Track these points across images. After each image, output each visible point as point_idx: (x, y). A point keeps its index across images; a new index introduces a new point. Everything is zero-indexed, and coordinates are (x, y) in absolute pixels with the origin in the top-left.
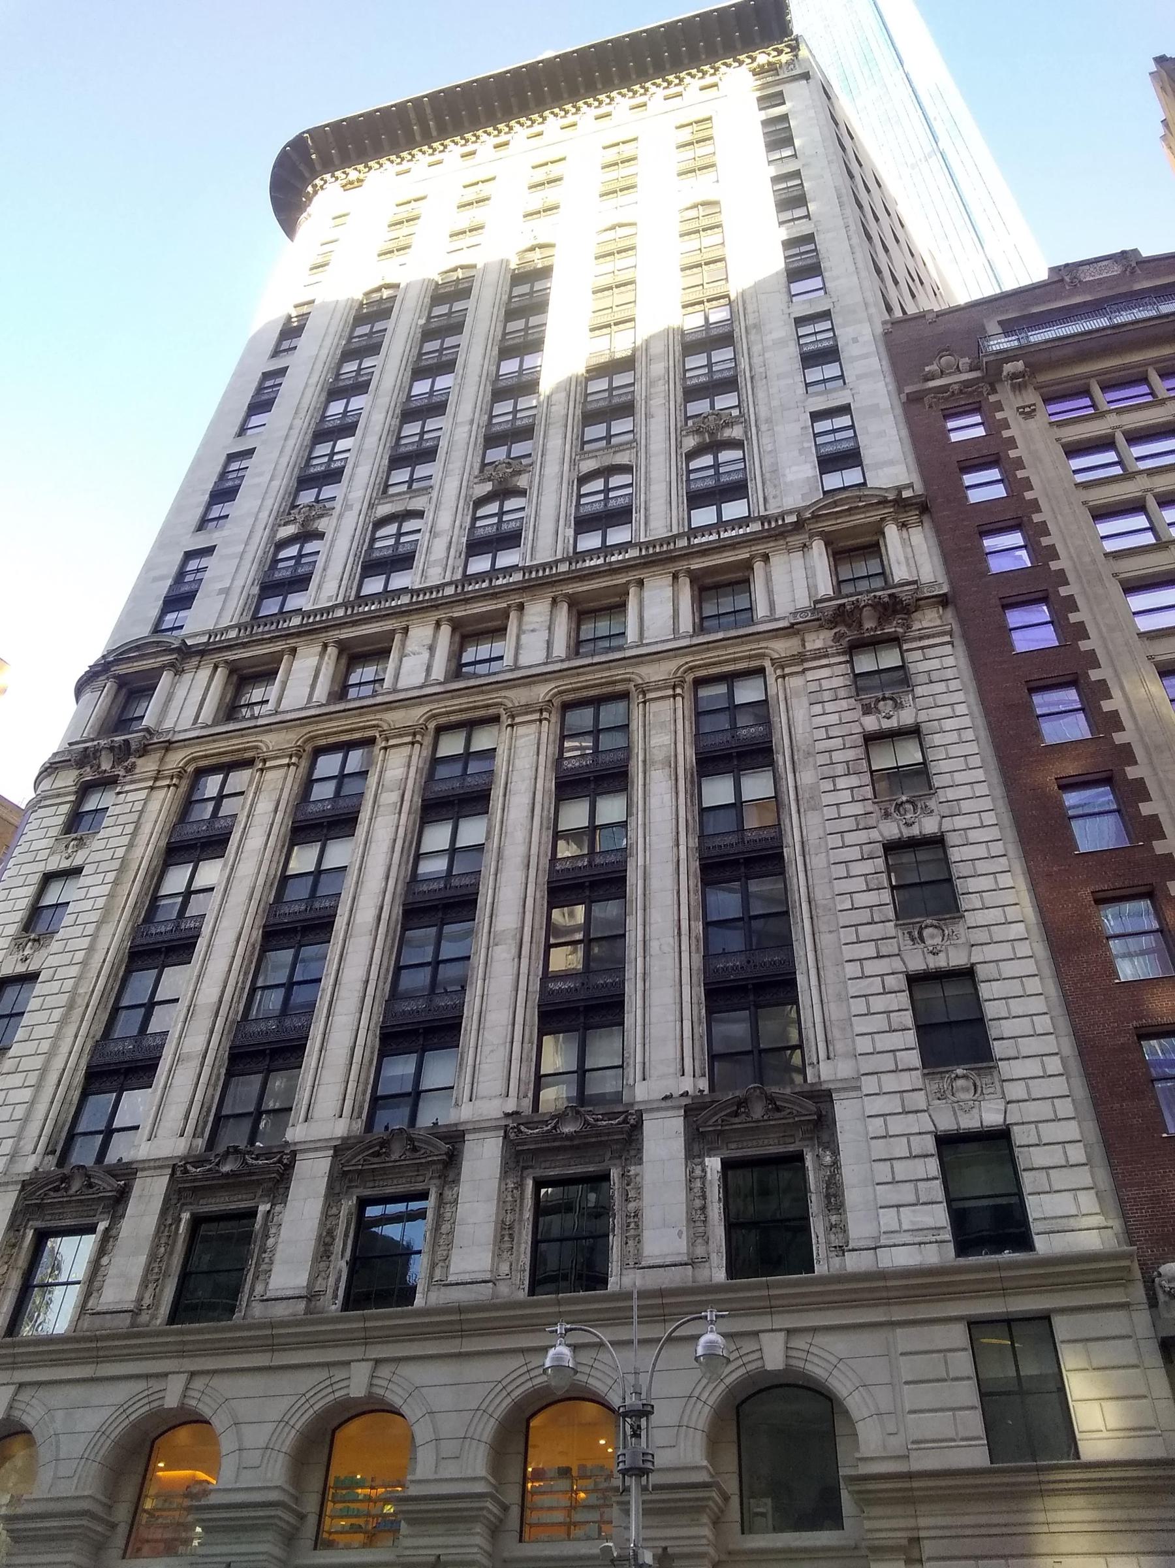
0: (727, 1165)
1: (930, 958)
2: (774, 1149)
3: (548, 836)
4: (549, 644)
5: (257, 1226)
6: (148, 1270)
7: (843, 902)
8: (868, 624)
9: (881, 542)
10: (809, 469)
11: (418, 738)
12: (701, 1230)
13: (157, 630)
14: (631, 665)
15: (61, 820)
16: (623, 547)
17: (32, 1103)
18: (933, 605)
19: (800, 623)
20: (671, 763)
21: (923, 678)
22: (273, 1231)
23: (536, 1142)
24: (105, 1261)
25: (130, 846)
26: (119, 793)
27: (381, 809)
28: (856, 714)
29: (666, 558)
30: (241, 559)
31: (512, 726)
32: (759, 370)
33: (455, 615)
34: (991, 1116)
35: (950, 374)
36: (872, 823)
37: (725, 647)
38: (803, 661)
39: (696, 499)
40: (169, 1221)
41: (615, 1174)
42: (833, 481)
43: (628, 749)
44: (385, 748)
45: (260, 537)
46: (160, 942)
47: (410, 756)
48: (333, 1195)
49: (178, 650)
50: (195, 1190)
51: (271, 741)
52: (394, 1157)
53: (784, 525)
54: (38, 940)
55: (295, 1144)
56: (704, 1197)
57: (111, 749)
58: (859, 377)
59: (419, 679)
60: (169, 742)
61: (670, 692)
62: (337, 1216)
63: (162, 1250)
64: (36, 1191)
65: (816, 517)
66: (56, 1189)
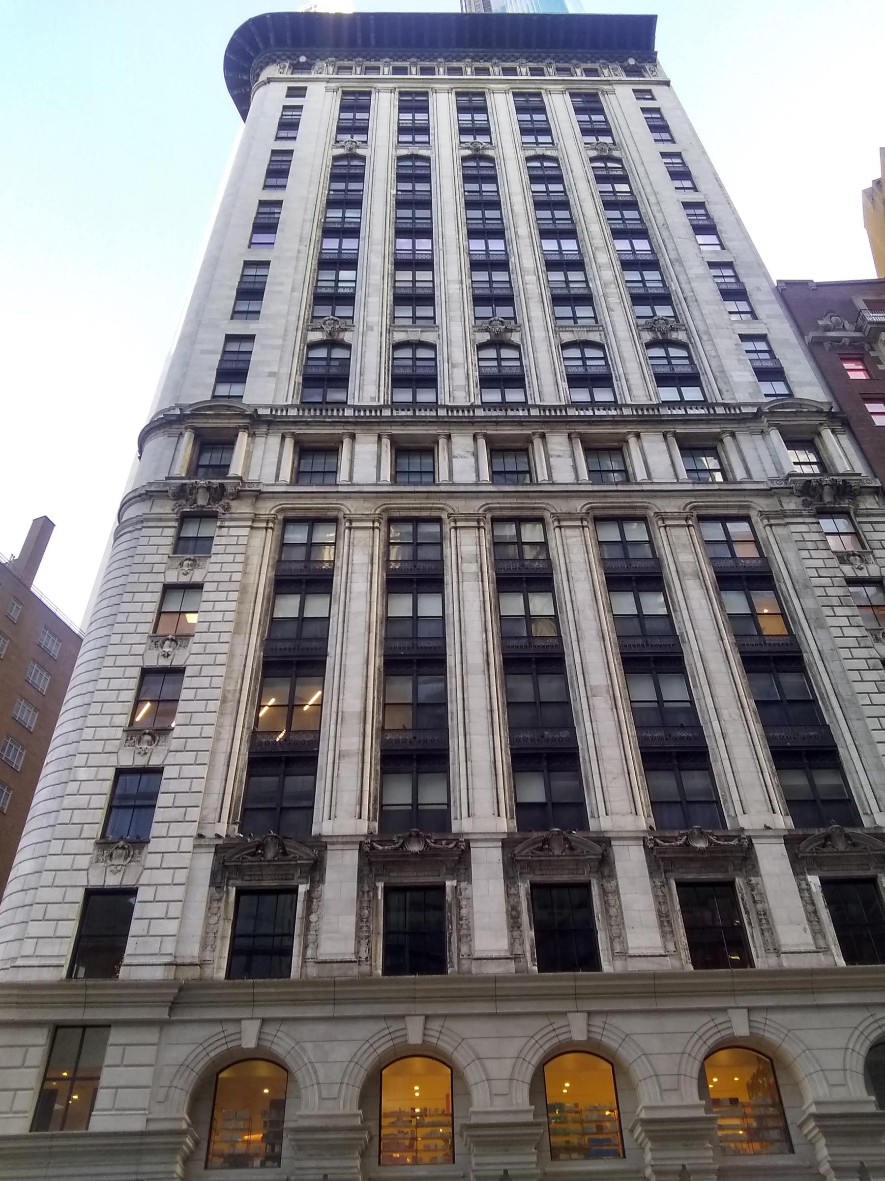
0: (824, 882)
2: (857, 873)
3: (610, 618)
5: (449, 897)
6: (359, 929)
7: (862, 699)
8: (827, 499)
9: (817, 441)
10: (749, 376)
12: (817, 928)
13: (214, 397)
14: (647, 497)
15: (170, 541)
16: (606, 405)
17: (208, 779)
18: (870, 494)
19: (777, 488)
20: (699, 575)
21: (878, 545)
22: (463, 903)
23: (674, 853)
24: (313, 918)
25: (245, 573)
26: (221, 527)
27: (465, 576)
28: (836, 562)
29: (657, 421)
30: (282, 351)
31: (560, 527)
33: (489, 432)
35: (839, 330)
36: (870, 644)
37: (720, 496)
38: (786, 517)
39: (662, 380)
40: (366, 888)
41: (739, 881)
42: (767, 387)
43: (657, 560)
46: (293, 658)
47: (479, 538)
48: (510, 879)
49: (250, 416)
50: (385, 865)
51: (351, 507)
52: (557, 852)
53: (741, 413)
54: (175, 641)
55: (467, 834)
56: (813, 904)
57: (208, 488)
58: (769, 317)
59: (472, 478)
60: (260, 492)
62: (517, 895)
63: (366, 912)
64: (232, 857)
65: (771, 413)
66: (254, 854)
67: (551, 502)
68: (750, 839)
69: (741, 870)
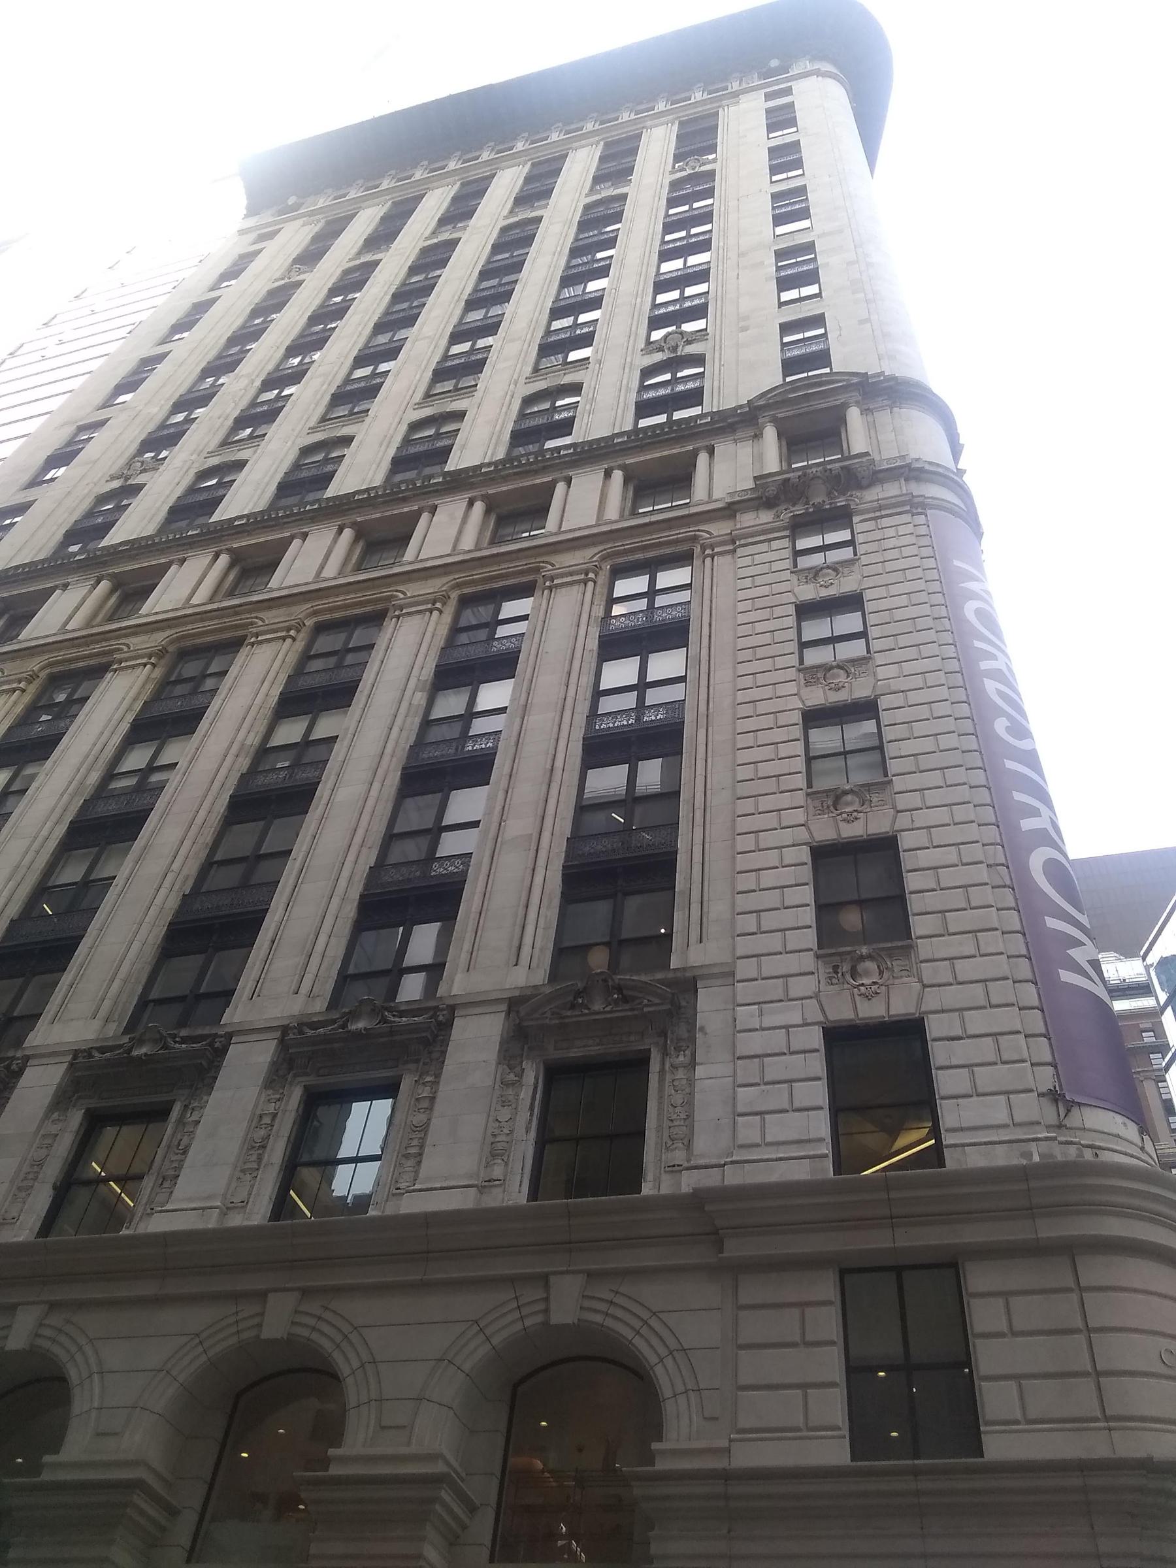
1: (842, 825)
11: (292, 633)
34: (900, 1003)
44: (253, 644)
68: (452, 1009)
69: (417, 1061)
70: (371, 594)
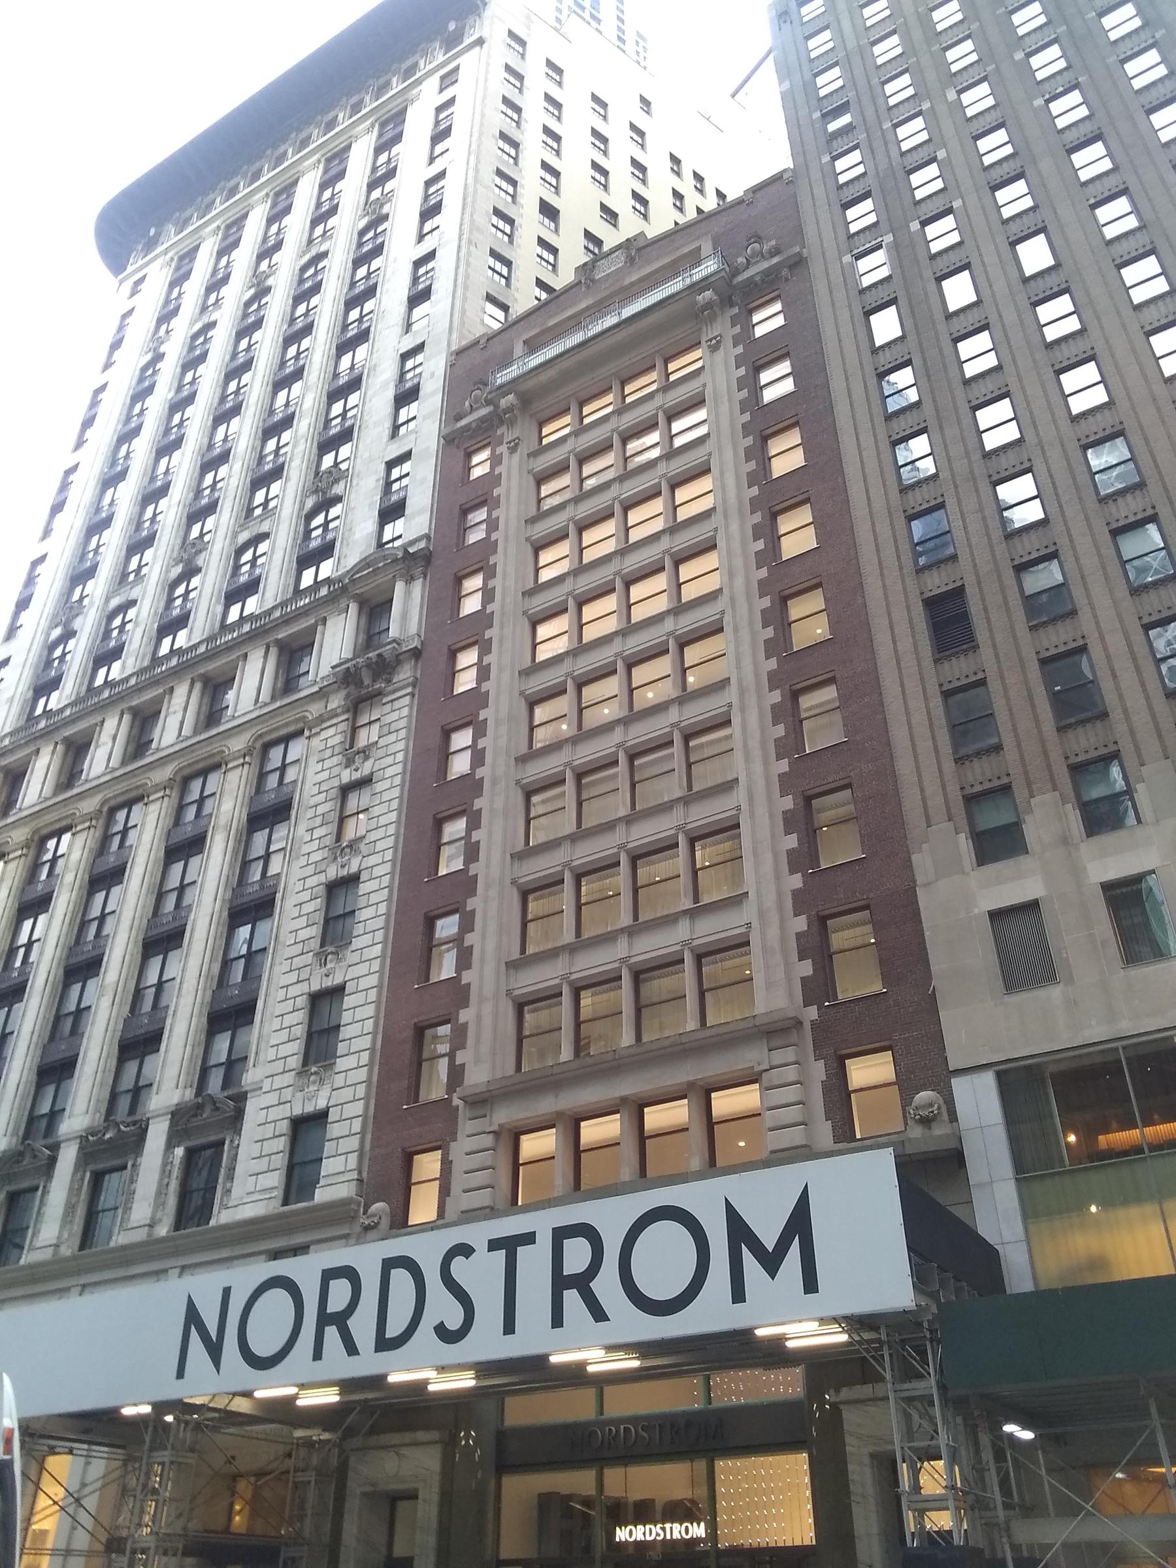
4: (182, 723)
8: (367, 682)
11: (94, 823)
32: (366, 417)
33: (134, 703)
34: (321, 1104)
35: (477, 409)
36: (323, 868)
38: (323, 722)
45: (39, 640)
61: (242, 761)
65: (352, 581)
67: (151, 775)
70: (135, 782)
